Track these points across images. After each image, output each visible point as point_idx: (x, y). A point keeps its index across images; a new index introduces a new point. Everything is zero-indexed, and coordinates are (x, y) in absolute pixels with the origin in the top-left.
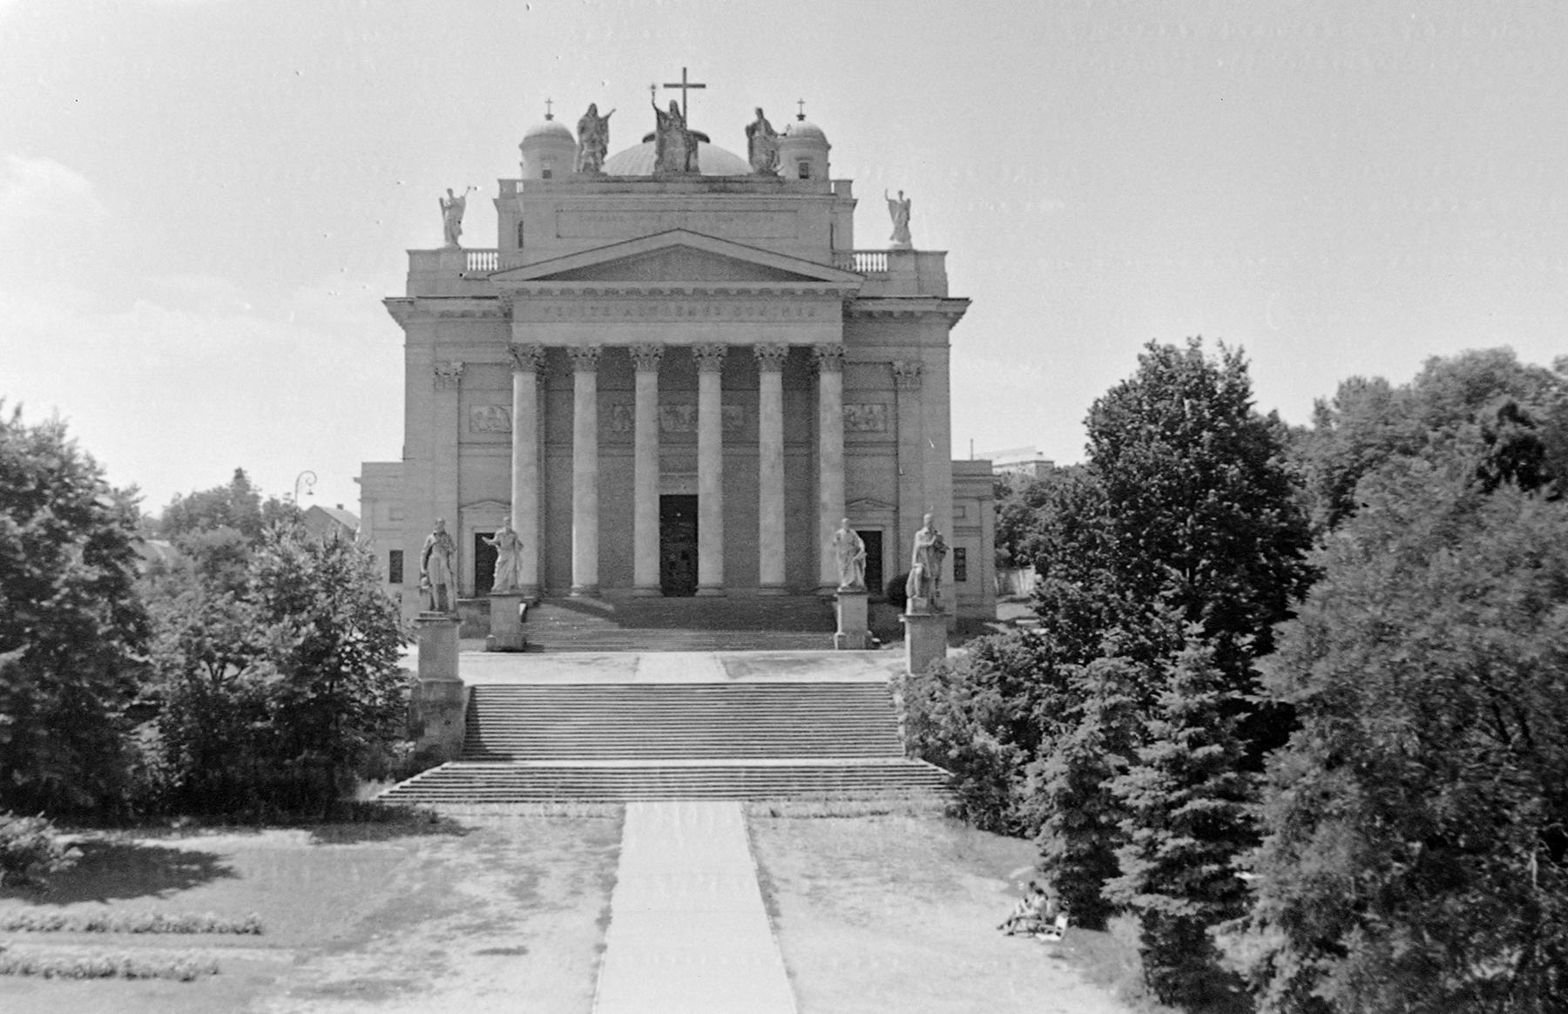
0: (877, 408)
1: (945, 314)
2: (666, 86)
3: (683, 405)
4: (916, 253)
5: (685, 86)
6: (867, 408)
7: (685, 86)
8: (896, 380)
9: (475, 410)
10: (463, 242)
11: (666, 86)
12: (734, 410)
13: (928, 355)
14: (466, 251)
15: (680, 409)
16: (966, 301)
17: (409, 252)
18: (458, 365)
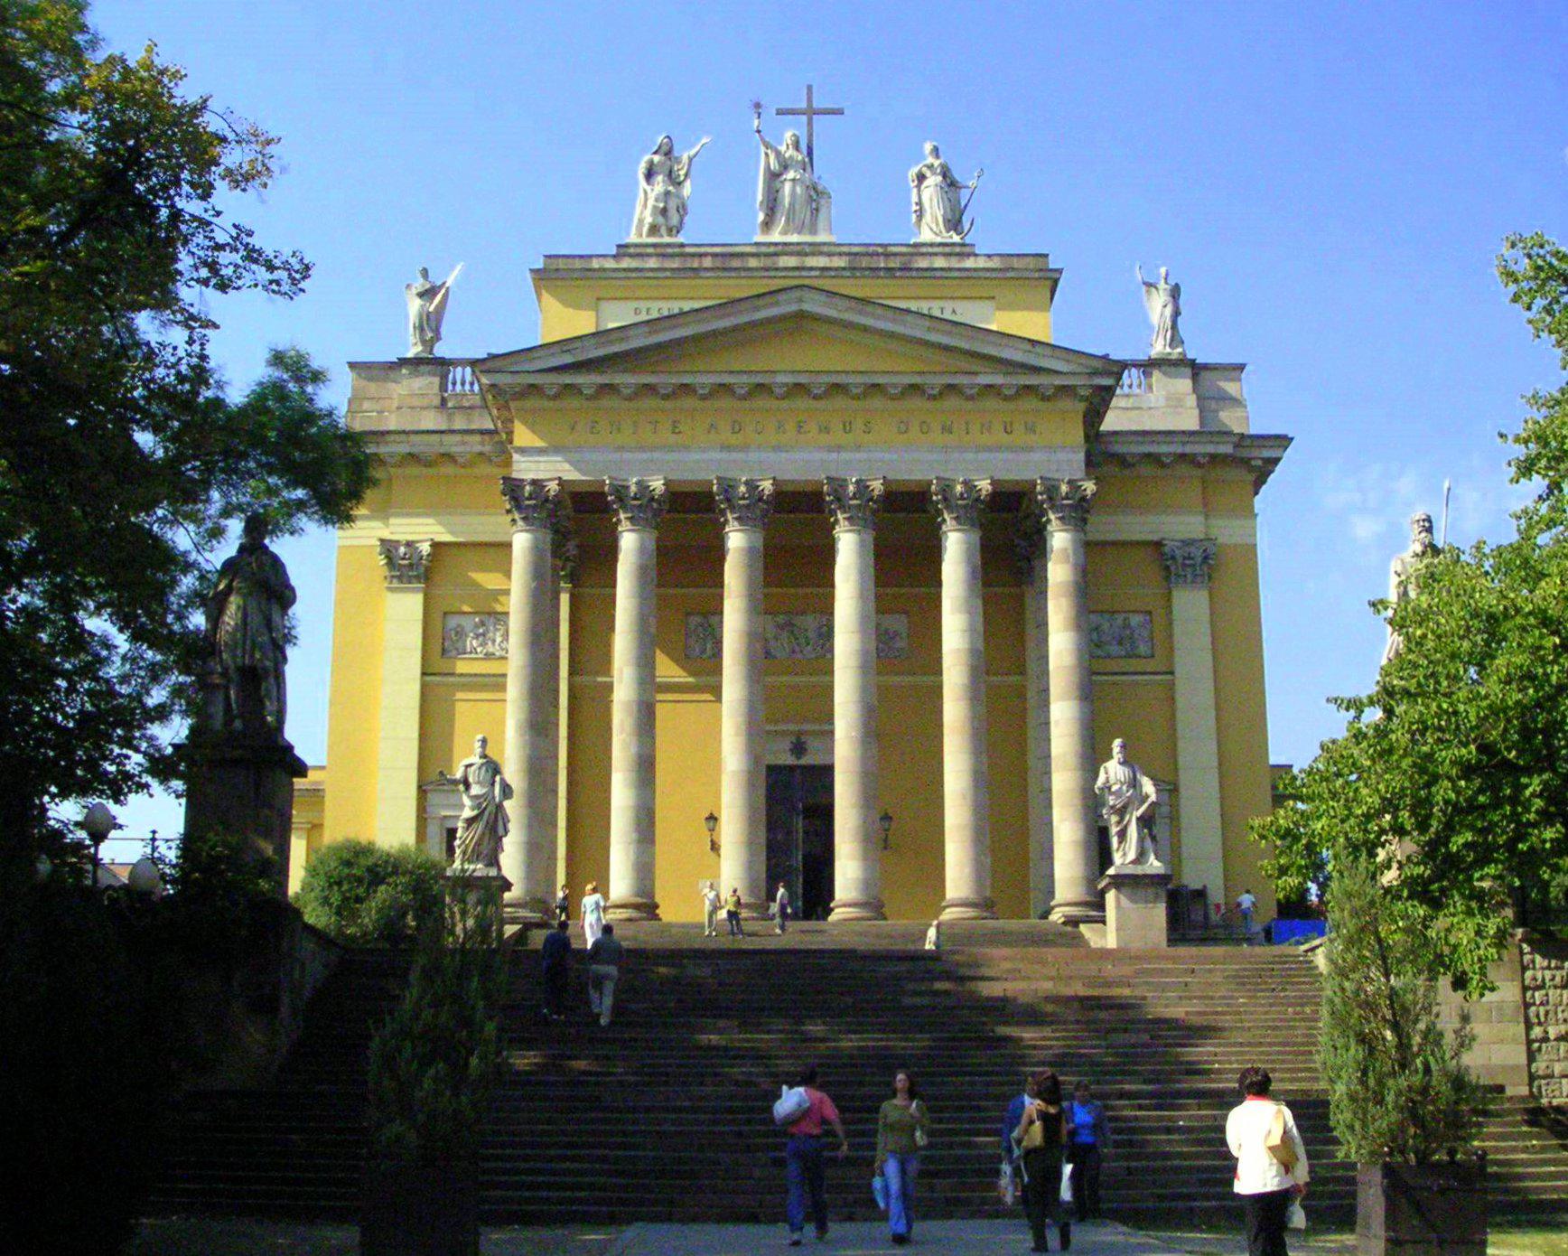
0: (1135, 620)
1: (1245, 463)
2: (780, 112)
3: (803, 613)
4: (1193, 364)
5: (811, 112)
6: (1119, 619)
7: (811, 112)
8: (1167, 568)
9: (452, 622)
10: (441, 350)
11: (780, 112)
12: (898, 623)
13: (1226, 531)
14: (443, 364)
15: (798, 620)
16: (1284, 441)
17: (352, 365)
18: (425, 548)
